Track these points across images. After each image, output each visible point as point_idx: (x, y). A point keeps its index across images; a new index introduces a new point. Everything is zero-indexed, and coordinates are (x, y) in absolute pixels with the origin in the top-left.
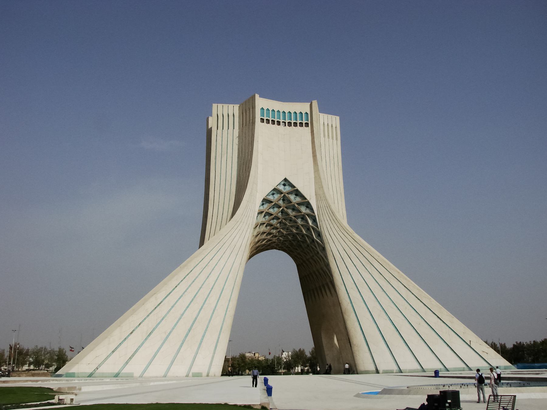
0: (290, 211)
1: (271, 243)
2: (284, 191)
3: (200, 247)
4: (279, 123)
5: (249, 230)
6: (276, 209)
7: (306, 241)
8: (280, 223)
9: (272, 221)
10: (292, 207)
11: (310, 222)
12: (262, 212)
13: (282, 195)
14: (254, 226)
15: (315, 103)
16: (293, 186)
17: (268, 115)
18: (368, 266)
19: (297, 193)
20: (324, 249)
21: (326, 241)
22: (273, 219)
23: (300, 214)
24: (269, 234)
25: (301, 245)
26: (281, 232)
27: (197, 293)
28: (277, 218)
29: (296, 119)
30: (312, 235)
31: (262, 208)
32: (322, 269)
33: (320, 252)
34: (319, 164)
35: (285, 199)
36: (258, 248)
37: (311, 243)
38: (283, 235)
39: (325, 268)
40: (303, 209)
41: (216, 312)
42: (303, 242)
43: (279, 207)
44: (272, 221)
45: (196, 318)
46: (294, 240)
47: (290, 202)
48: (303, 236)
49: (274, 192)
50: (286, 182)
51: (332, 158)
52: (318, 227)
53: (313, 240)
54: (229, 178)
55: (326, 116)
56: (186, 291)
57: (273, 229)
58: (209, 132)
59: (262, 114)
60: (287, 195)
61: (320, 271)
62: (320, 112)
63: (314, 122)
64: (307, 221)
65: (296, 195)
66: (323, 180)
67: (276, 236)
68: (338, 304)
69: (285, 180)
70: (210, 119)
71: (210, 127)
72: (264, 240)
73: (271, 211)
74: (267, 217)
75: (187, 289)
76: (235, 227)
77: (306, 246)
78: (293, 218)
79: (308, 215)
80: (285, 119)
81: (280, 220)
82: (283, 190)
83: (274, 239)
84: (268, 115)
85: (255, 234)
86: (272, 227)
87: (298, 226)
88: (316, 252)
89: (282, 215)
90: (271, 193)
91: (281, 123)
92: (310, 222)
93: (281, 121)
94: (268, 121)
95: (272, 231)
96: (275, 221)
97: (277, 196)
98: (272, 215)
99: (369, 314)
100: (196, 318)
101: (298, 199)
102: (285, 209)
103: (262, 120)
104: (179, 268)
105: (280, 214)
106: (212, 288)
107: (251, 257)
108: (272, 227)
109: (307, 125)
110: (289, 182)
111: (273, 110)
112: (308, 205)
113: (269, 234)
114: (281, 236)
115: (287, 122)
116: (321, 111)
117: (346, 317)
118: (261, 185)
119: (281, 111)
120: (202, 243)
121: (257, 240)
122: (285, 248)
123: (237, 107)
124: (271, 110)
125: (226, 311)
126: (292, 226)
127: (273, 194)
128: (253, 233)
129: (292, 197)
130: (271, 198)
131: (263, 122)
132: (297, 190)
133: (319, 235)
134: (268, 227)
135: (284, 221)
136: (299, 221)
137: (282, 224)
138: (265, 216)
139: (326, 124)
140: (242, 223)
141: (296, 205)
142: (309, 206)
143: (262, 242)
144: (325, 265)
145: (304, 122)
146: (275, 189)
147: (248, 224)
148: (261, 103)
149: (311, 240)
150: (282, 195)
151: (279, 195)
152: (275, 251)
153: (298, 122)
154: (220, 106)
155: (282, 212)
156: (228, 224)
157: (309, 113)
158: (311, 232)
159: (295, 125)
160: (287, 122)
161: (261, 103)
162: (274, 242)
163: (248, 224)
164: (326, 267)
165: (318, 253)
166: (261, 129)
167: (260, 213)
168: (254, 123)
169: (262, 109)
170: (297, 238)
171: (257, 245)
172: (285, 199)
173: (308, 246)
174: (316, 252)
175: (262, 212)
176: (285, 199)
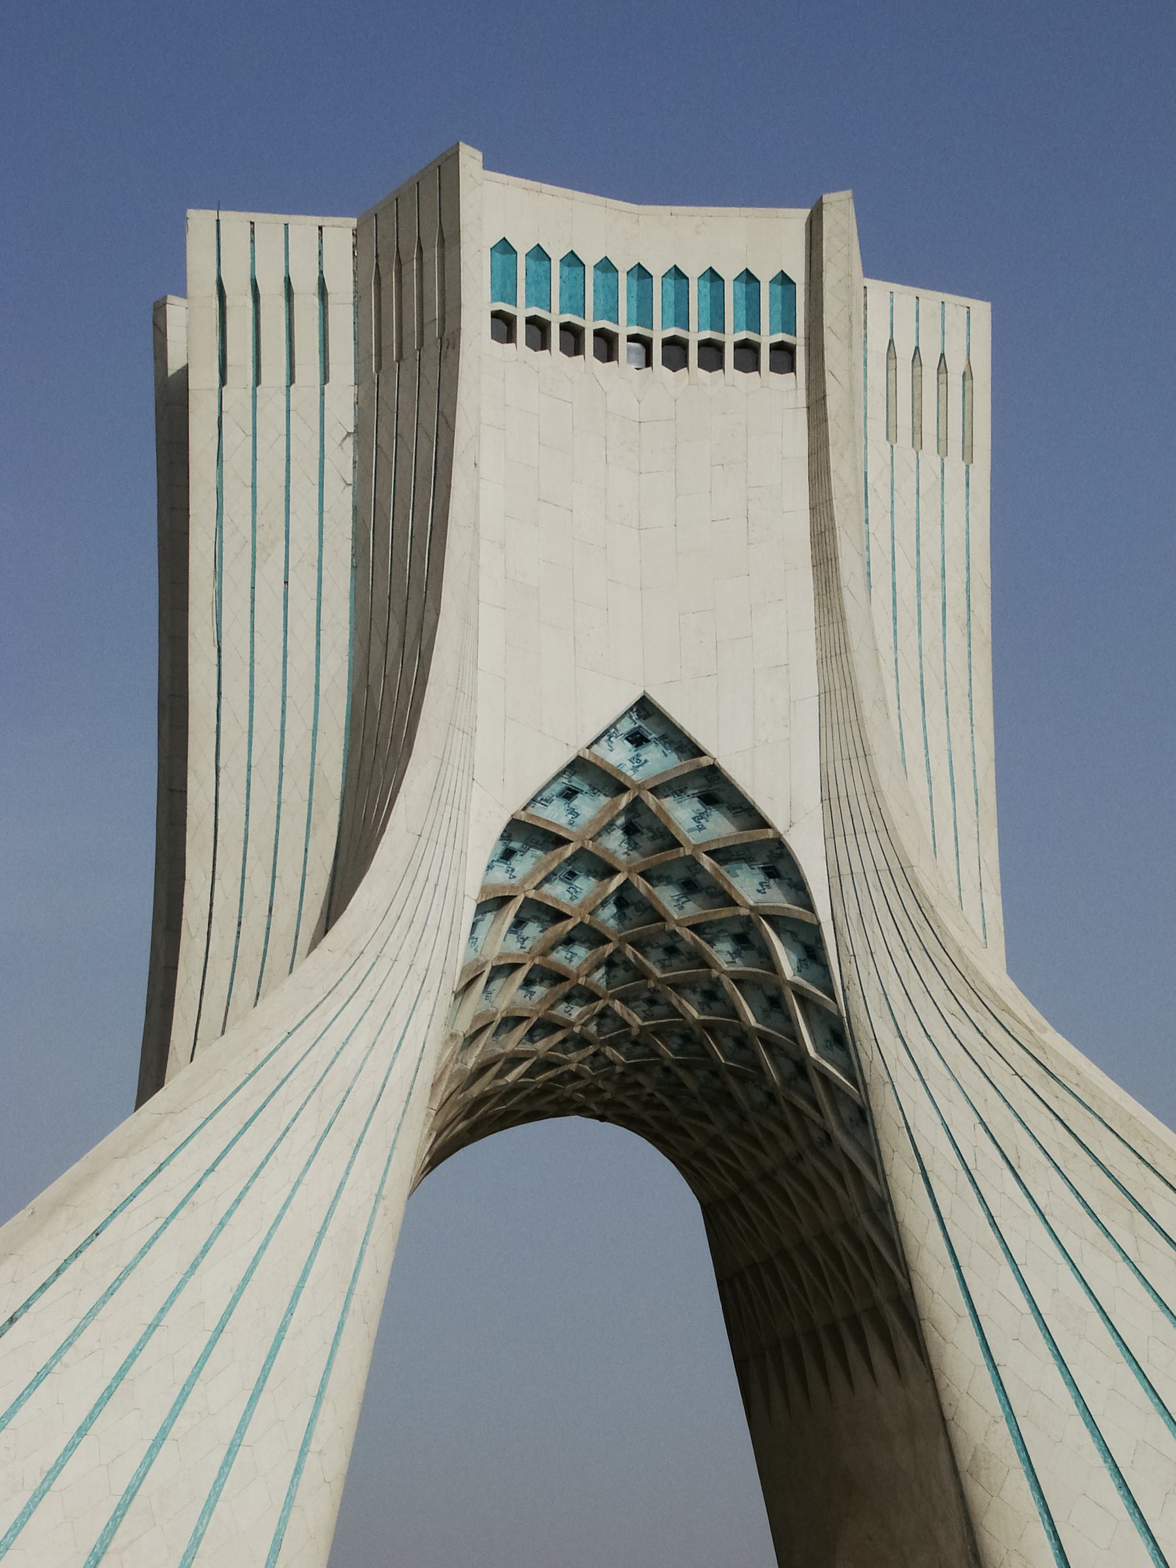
0: (666, 897)
1: (558, 1079)
2: (637, 777)
3: (140, 1102)
4: (607, 345)
5: (425, 1007)
6: (586, 885)
7: (759, 1067)
8: (610, 963)
9: (559, 956)
10: (680, 873)
11: (787, 962)
12: (503, 901)
13: (625, 800)
14: (454, 981)
15: (840, 212)
16: (687, 747)
17: (539, 292)
18: (1119, 1218)
19: (715, 788)
20: (862, 1117)
21: (873, 1071)
22: (568, 941)
23: (726, 912)
24: (546, 1026)
25: (729, 1095)
26: (616, 1017)
27: (133, 1356)
28: (593, 936)
29: (717, 320)
30: (796, 1037)
31: (500, 875)
32: (847, 1228)
33: (838, 1135)
34: (850, 612)
35: (643, 821)
36: (476, 1113)
37: (788, 1082)
38: (622, 1035)
39: (864, 1220)
40: (748, 887)
41: (242, 1455)
42: (742, 1078)
43: (606, 871)
44: (559, 956)
45: (131, 1492)
46: (686, 1066)
48: (742, 1039)
49: (576, 782)
50: (648, 720)
51: (930, 574)
52: (832, 996)
53: (801, 1067)
54: (300, 692)
55: (905, 295)
56: (68, 1343)
57: (568, 998)
58: (172, 400)
59: (504, 286)
60: (650, 800)
61: (841, 1240)
62: (869, 272)
63: (829, 340)
64: (767, 958)
65: (709, 800)
66: (869, 711)
67: (582, 1042)
68: (934, 1421)
69: (644, 707)
70: (176, 311)
71: (173, 366)
72: (514, 1060)
73: (557, 892)
74: (532, 930)
75: (77, 1332)
76: (347, 987)
77: (759, 1097)
78: (687, 935)
79: (774, 920)
80: (644, 317)
81: (609, 949)
82: (627, 769)
83: (575, 1059)
84: (539, 292)
85: (464, 1026)
86: (565, 987)
87: (717, 983)
88: (816, 1135)
89: (621, 916)
90: (557, 788)
91: (623, 345)
92: (787, 962)
93: (623, 330)
94: (539, 330)
95: (561, 1010)
96: (581, 952)
97: (589, 807)
98: (559, 916)
99: (1111, 1484)
100: (131, 1492)
101: (720, 827)
102: (641, 884)
103: (503, 326)
104: (22, 1215)
105: (611, 910)
106: (219, 1330)
107: (437, 1157)
108: (565, 987)
109: (783, 356)
110: (663, 719)
111: (572, 260)
112: (778, 862)
113: (546, 1026)
114: (613, 1043)
115: (658, 335)
116: (881, 261)
117: (977, 1493)
118: (504, 730)
119: (624, 265)
120: (152, 1076)
121: (471, 1062)
122: (635, 1108)
123: (340, 234)
124: (556, 254)
125: (303, 1453)
126: (677, 986)
127: (569, 794)
128: (451, 1020)
129: (682, 813)
130: (555, 815)
131: (510, 338)
132: (714, 771)
133: (838, 1035)
134: (540, 990)
135: (629, 951)
136: (722, 954)
137: (620, 973)
138: (519, 923)
139: (904, 353)
140: (384, 965)
141: (707, 862)
142: (782, 866)
143: (501, 1074)
144: (868, 1209)
145: (766, 339)
146: (578, 766)
147: (420, 967)
148: (497, 207)
149: (789, 1068)
150: (625, 800)
151: (603, 800)
152: (575, 1122)
153: (730, 338)
154: (235, 222)
155: (623, 898)
156: (305, 967)
157: (798, 275)
158: (790, 1019)
159: (712, 355)
160: (658, 335)
161: (497, 207)
162: (575, 1076)
163: (420, 967)
164: (874, 1220)
165: (828, 1138)
166: (496, 384)
167: (494, 903)
168: (449, 342)
169: (504, 248)
170: (706, 1053)
171: (475, 1091)
172: (638, 824)
173: (771, 1097)
174: (816, 1135)
175: (503, 901)
176: (638, 824)
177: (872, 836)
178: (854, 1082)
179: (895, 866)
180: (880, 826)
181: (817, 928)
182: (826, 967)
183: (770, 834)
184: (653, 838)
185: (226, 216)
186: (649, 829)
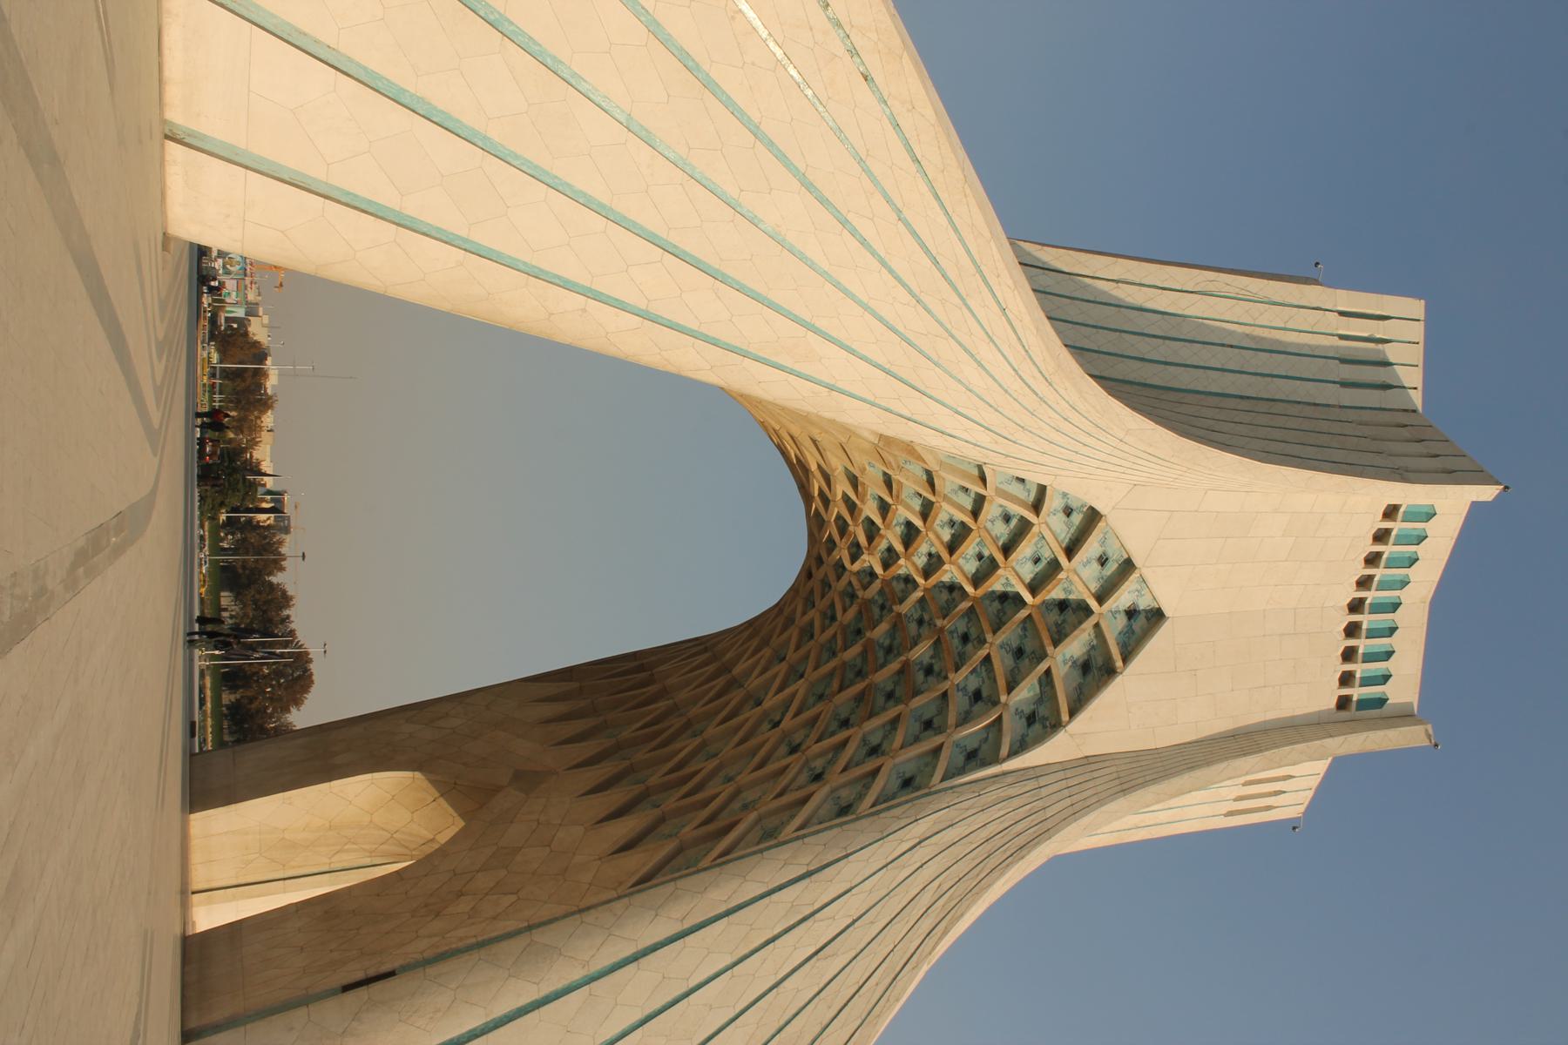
19: (1096, 672)
35: (1070, 616)
113: (910, 535)
129: (1076, 645)
132: (1110, 672)
172: (1071, 612)
177: (1068, 802)
179: (1048, 824)
180: (1077, 807)
181: (995, 760)
182: (962, 771)
183: (1065, 717)
184: (1057, 625)
185: (1420, 327)
186: (1064, 621)
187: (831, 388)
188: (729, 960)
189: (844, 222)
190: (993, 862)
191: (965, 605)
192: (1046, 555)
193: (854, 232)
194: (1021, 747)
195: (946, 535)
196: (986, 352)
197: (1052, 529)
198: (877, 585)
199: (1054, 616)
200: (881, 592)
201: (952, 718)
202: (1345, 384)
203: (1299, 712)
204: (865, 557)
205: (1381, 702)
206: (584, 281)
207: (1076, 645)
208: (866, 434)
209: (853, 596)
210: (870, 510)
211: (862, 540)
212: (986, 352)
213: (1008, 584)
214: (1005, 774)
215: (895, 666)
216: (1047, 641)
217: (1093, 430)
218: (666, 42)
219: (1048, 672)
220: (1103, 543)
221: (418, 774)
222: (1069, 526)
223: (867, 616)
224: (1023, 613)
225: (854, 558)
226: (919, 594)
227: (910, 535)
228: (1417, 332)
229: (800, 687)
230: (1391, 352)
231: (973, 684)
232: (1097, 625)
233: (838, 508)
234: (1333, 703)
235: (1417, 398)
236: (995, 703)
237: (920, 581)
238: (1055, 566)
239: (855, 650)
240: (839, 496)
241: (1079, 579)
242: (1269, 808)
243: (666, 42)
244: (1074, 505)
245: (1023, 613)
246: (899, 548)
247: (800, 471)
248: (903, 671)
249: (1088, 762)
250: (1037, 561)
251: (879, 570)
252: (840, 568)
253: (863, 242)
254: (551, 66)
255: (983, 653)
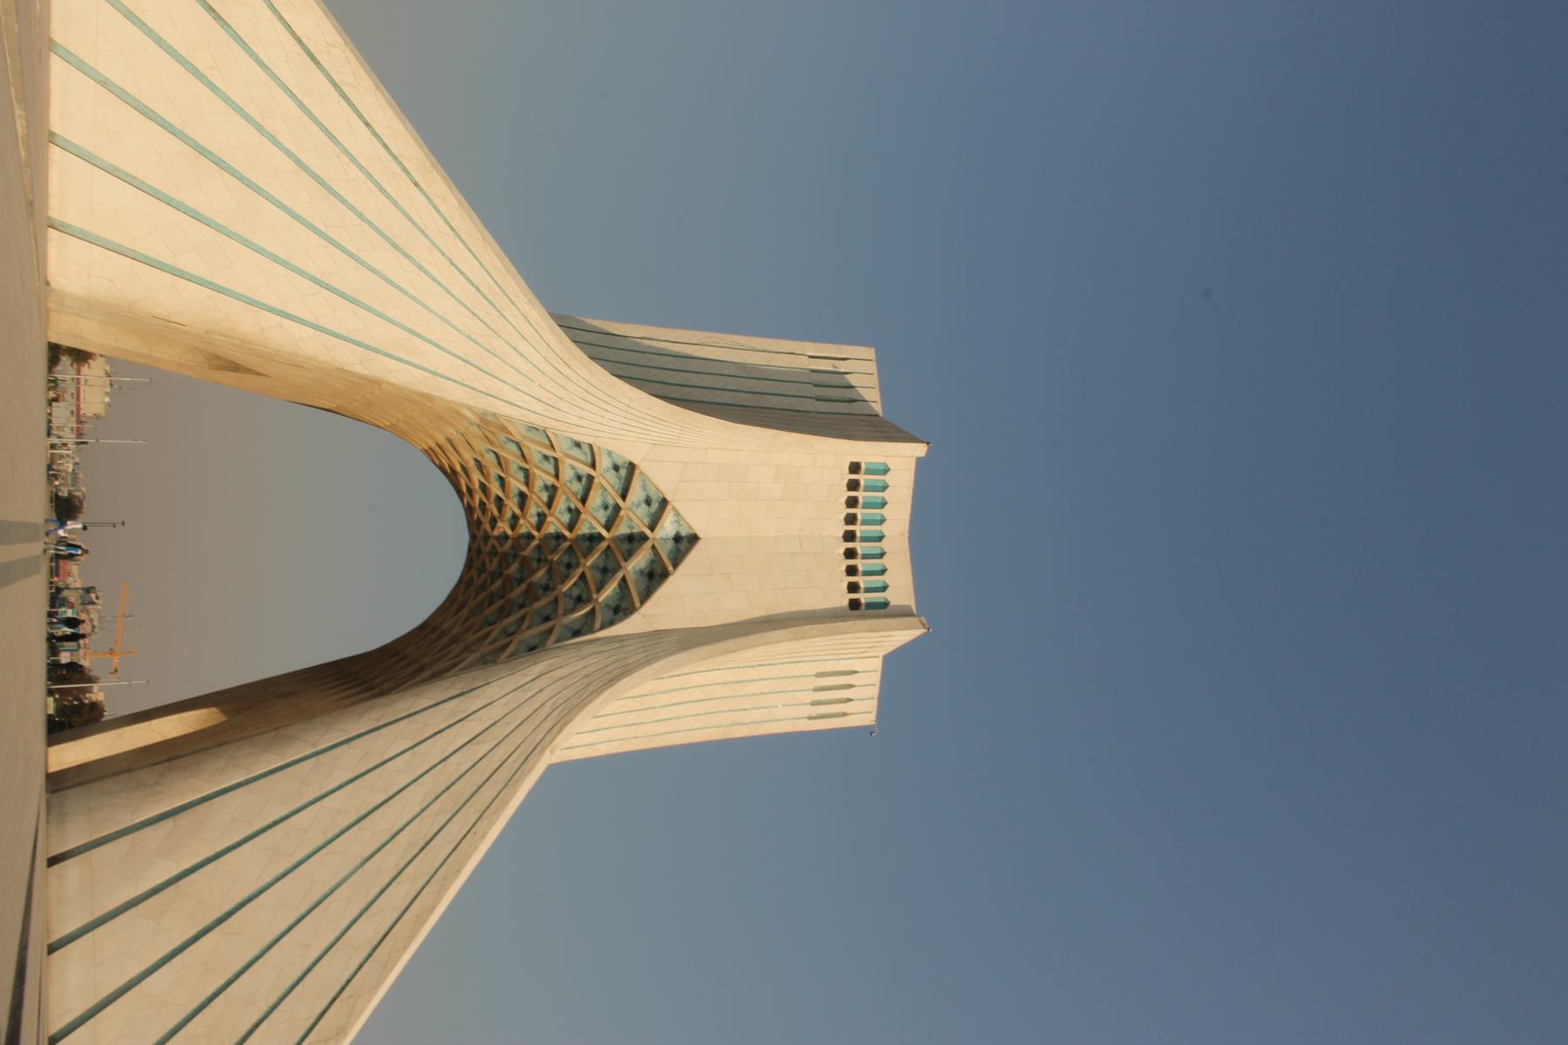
10: (611, 565)
19: (655, 576)
20: (488, 660)
23: (593, 588)
35: (635, 544)
47: (628, 555)
50: (685, 543)
99: (276, 817)
112: (622, 609)
113: (523, 497)
129: (640, 560)
132: (665, 575)
172: (634, 541)
178: (512, 655)
181: (592, 631)
183: (637, 604)
187: (435, 374)
188: (410, 744)
189: (420, 267)
190: (591, 689)
191: (566, 544)
192: (611, 502)
193: (427, 273)
194: (611, 623)
195: (545, 496)
196: (523, 346)
197: (607, 481)
198: (509, 543)
199: (626, 546)
200: (513, 547)
201: (561, 611)
202: (819, 399)
203: (817, 607)
204: (499, 524)
205: (885, 605)
206: (279, 306)
207: (640, 560)
208: (468, 414)
209: (496, 554)
210: (495, 489)
211: (496, 513)
212: (523, 346)
213: (592, 527)
214: (598, 639)
215: (523, 587)
216: (620, 558)
217: (605, 397)
218: (307, 170)
219: (624, 579)
220: (644, 488)
221: (214, 710)
222: (619, 478)
223: (505, 560)
224: (604, 545)
225: (493, 528)
226: (536, 542)
227: (523, 497)
228: (872, 367)
229: (465, 612)
230: (852, 380)
231: (576, 593)
232: (653, 547)
233: (478, 496)
234: (846, 603)
235: (878, 408)
236: (589, 600)
237: (535, 533)
238: (617, 508)
239: (498, 583)
240: (477, 485)
241: (634, 518)
242: (844, 714)
243: (307, 170)
244: (619, 463)
245: (604, 545)
246: (518, 512)
247: (452, 476)
248: (527, 591)
249: (658, 634)
250: (606, 507)
251: (509, 532)
252: (487, 537)
253: (434, 279)
254: (250, 185)
255: (579, 571)
